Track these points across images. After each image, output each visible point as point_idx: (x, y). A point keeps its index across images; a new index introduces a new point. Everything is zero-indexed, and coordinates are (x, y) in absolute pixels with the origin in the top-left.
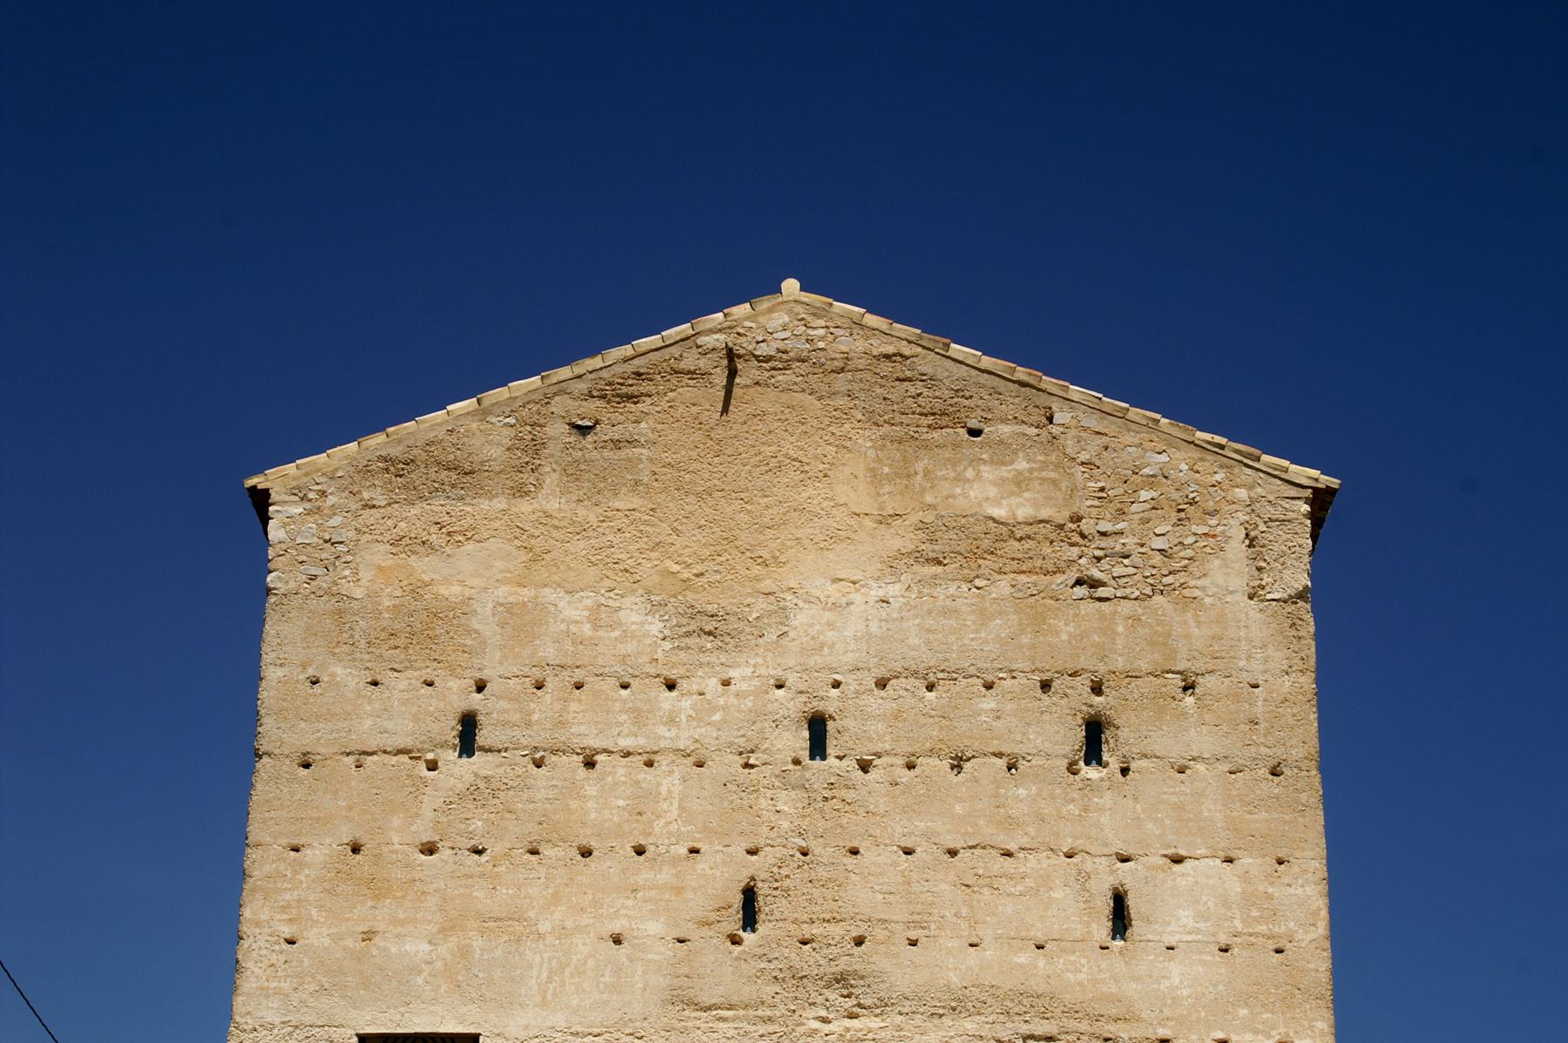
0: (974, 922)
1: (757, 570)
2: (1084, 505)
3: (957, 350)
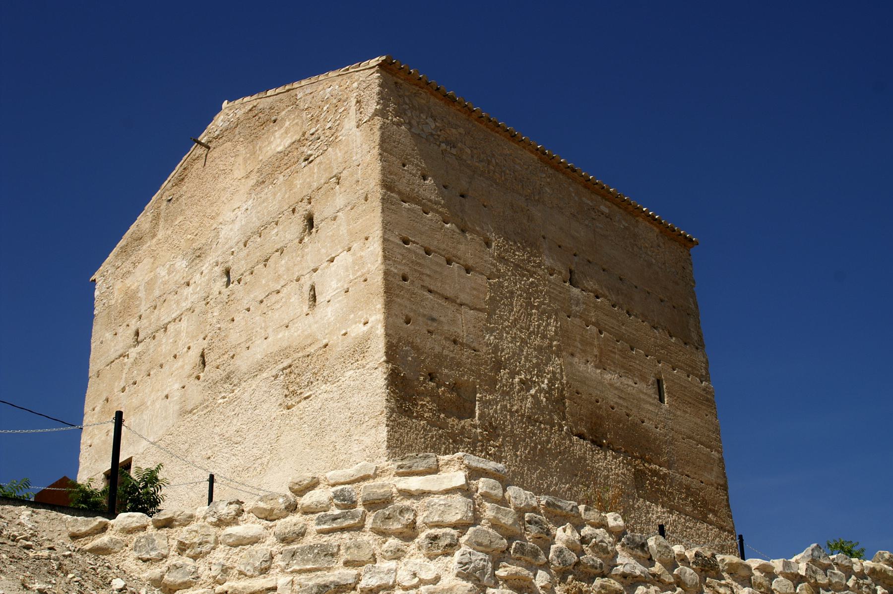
0: (265, 329)
1: (212, 222)
2: (305, 128)
3: (270, 93)
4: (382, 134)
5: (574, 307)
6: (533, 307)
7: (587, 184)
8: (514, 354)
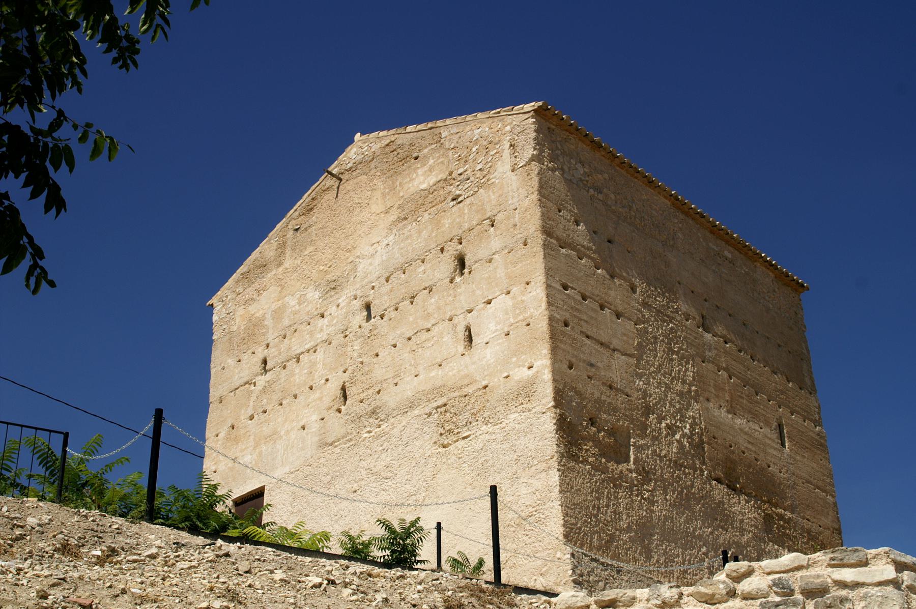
0: (416, 366)
1: (348, 254)
2: (452, 167)
3: (409, 129)
4: (540, 179)
5: (707, 353)
6: (674, 352)
7: (714, 230)
8: (660, 399)
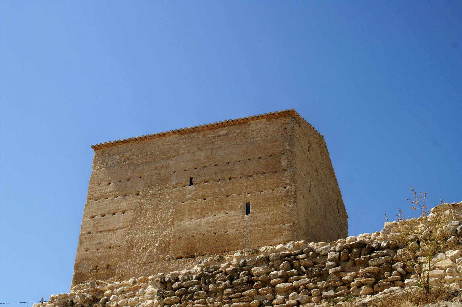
8: (142, 238)
